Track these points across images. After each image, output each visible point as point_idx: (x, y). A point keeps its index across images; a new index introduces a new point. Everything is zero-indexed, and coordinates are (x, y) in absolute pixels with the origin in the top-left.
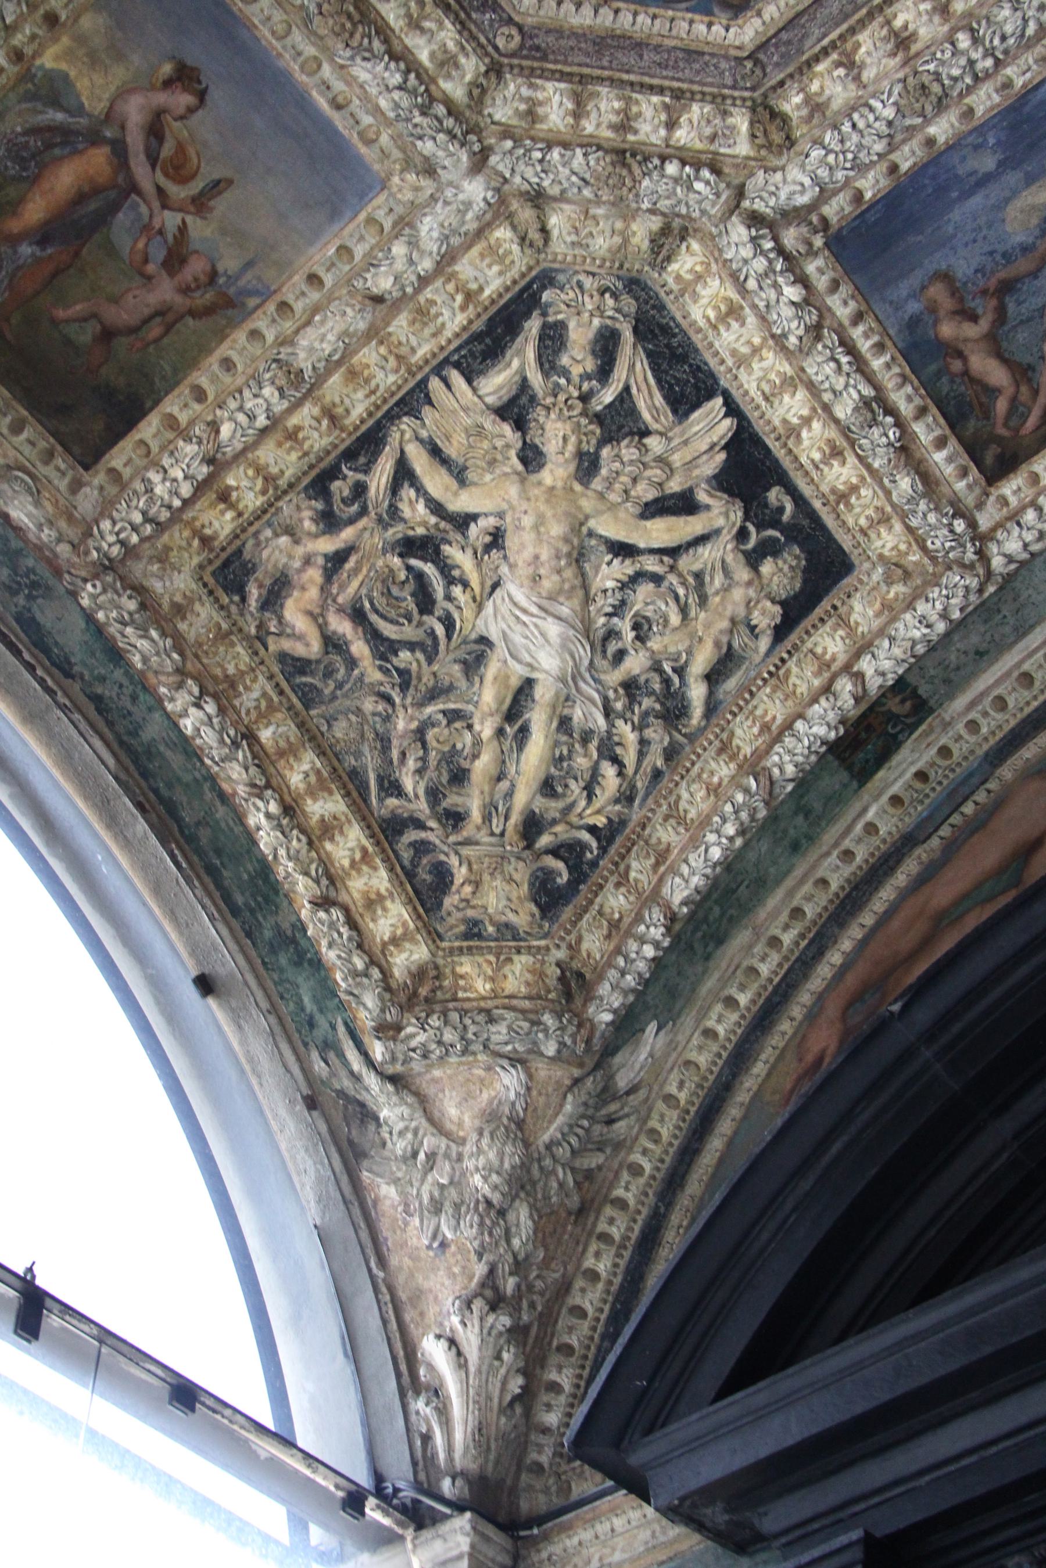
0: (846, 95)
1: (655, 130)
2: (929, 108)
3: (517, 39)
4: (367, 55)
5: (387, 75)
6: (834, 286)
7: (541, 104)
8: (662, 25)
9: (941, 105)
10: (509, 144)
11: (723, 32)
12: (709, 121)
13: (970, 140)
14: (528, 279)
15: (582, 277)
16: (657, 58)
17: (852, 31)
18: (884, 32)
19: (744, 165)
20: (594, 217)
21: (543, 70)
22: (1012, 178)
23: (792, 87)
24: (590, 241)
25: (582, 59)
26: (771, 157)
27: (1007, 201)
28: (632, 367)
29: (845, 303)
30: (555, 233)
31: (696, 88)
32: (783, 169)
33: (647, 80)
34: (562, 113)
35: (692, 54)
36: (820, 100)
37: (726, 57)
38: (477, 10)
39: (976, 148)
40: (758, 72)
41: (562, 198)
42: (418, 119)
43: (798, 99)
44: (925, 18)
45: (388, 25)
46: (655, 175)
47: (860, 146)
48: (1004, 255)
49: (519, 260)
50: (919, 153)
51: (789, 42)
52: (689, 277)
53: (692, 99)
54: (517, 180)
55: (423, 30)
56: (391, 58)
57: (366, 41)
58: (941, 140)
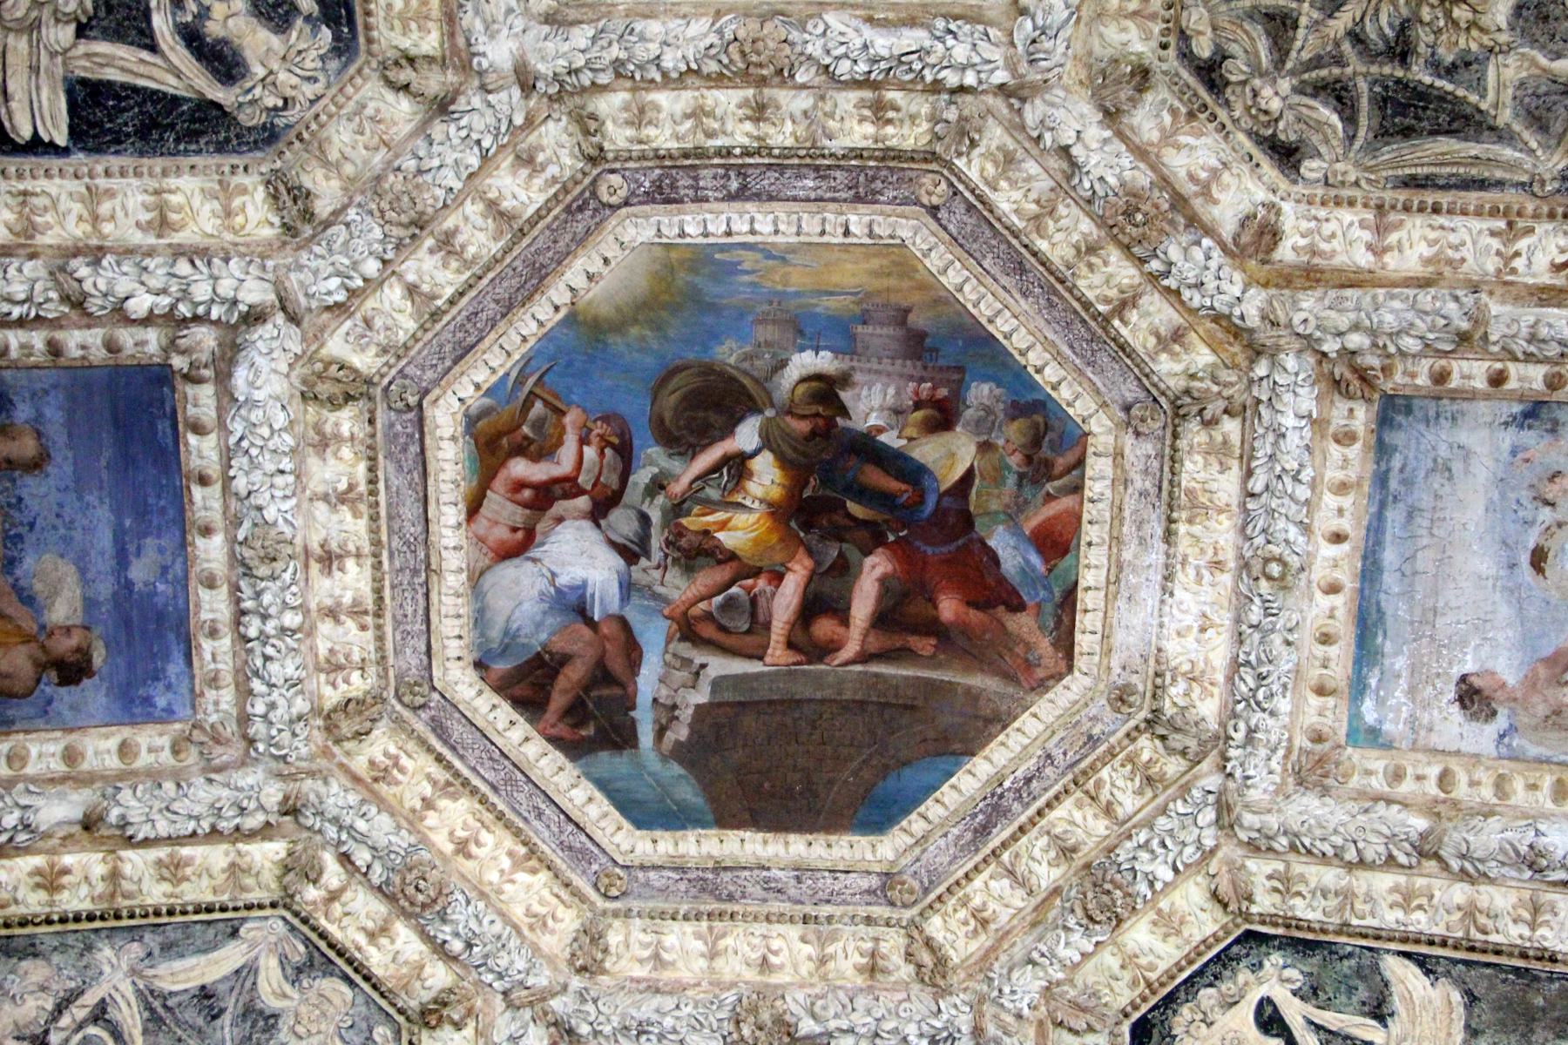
0: (316, 478)
1: (419, 272)
2: (247, 553)
3: (605, 198)
4: (713, 51)
5: (679, 55)
6: (112, 347)
7: (530, 177)
8: (512, 343)
9: (236, 561)
10: (519, 120)
11: (461, 395)
12: (388, 329)
13: (178, 567)
14: (360, 28)
15: (319, 88)
16: (484, 316)
17: (374, 518)
18: (351, 547)
19: (318, 336)
20: (377, 149)
21: (558, 202)
22: (105, 589)
23: (361, 431)
24: (354, 125)
25: (540, 244)
26: (305, 371)
27: (82, 571)
28: (178, 74)
29: (83, 347)
30: (390, 96)
31: (429, 335)
32: (287, 376)
33: (473, 293)
34: (507, 193)
35: (464, 352)
36: (328, 450)
37: (436, 382)
38: (660, 179)
39: (165, 570)
40: (400, 405)
41: (422, 129)
42: (616, 52)
43: (345, 430)
44: (338, 592)
45: (718, 87)
46: (377, 247)
47: (254, 465)
48: (20, 537)
49: (389, 37)
50: (203, 513)
51: (405, 450)
52: (237, 202)
53: (422, 326)
54: (477, 102)
55: (687, 116)
56: (689, 70)
57: (726, 61)
58: (200, 542)
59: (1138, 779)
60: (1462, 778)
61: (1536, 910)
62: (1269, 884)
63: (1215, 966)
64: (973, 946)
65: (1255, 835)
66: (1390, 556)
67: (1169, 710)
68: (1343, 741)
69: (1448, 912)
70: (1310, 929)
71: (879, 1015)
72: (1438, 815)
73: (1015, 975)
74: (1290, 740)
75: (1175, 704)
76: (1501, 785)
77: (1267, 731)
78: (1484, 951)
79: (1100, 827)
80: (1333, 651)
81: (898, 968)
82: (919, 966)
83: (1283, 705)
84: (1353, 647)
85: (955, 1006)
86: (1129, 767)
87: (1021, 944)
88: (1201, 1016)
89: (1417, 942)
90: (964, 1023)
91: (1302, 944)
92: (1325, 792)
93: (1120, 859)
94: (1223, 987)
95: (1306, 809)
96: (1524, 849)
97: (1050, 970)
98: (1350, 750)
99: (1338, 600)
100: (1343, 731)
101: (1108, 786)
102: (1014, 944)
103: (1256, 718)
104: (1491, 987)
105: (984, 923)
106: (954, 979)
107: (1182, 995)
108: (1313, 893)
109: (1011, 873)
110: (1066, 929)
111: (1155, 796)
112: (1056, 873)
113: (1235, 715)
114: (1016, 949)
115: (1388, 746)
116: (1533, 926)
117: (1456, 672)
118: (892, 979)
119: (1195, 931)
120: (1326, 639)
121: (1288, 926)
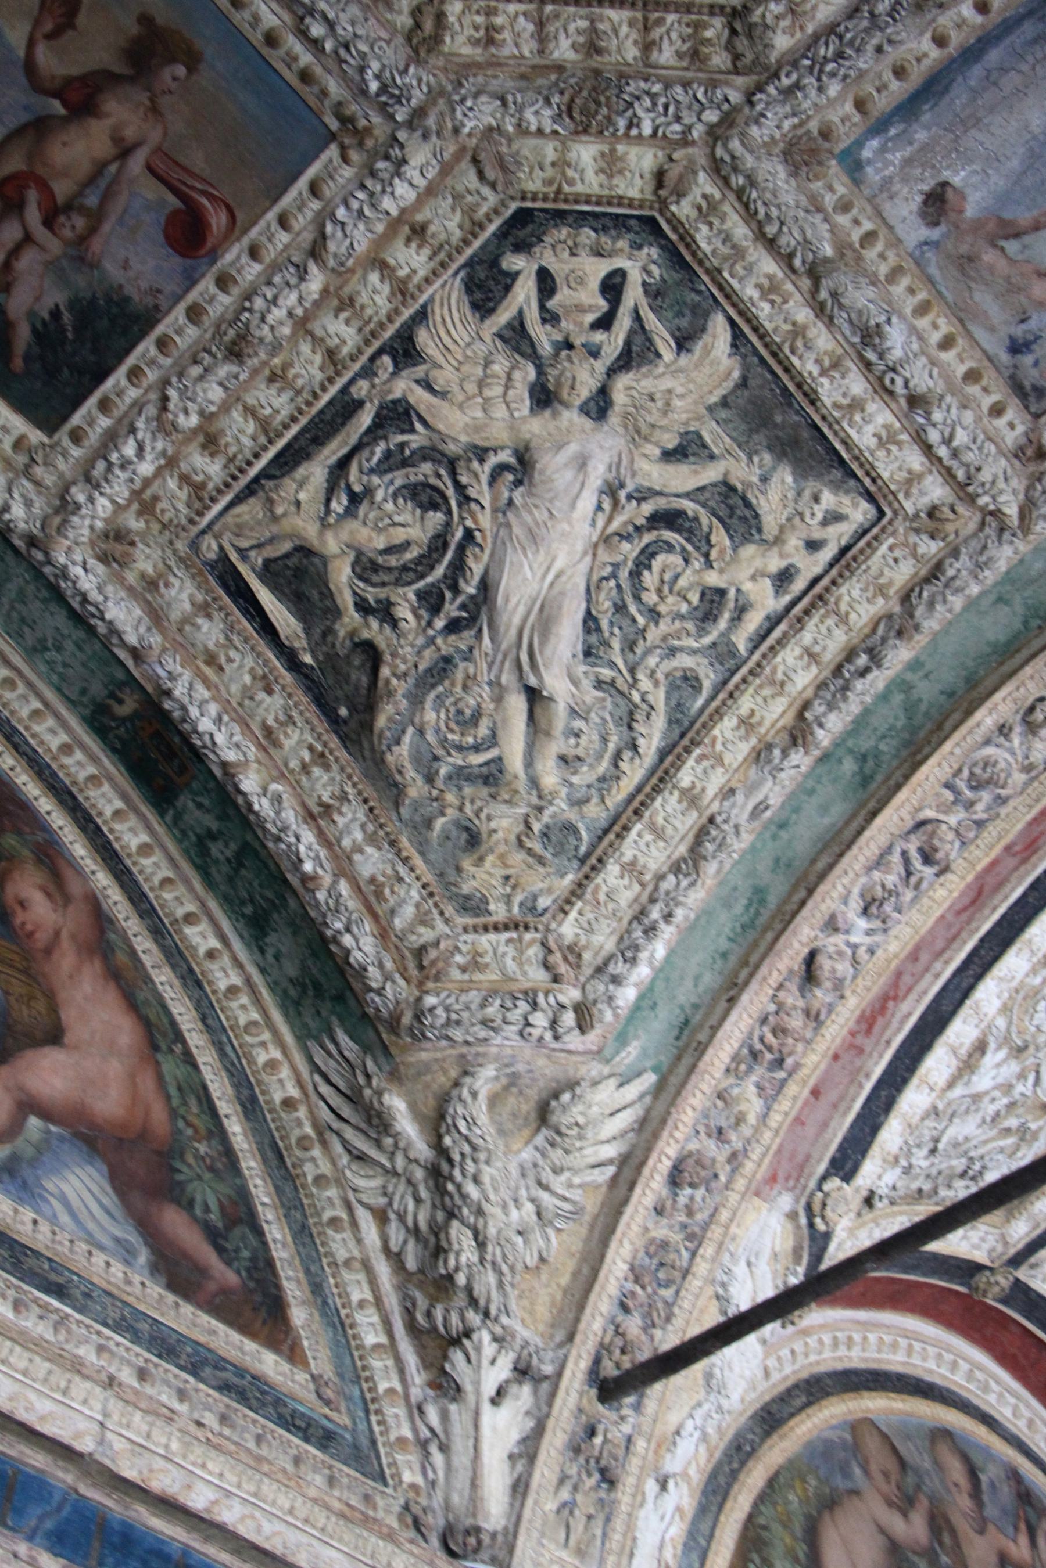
59: (688, 45)
60: (879, 246)
61: (836, 365)
62: (699, 199)
63: (611, 221)
64: (467, 50)
65: (727, 159)
66: (994, 56)
67: (755, 17)
68: (837, 151)
69: (785, 321)
70: (694, 254)
71: (360, 32)
72: (843, 255)
73: (484, 98)
74: (809, 117)
75: (763, 16)
76: (895, 273)
77: (806, 97)
78: (780, 362)
79: (632, 53)
80: (895, 85)
81: (400, 12)
82: (418, 26)
83: (834, 89)
84: (906, 96)
85: (420, 80)
86: (690, 31)
87: (502, 81)
88: (570, 243)
89: (748, 321)
90: (418, 97)
91: (680, 256)
92: (794, 173)
93: (628, 89)
94: (604, 239)
95: (775, 174)
96: (872, 323)
97: (507, 119)
98: (834, 162)
99: (935, 53)
100: (842, 145)
101: (663, 29)
102: (495, 77)
103: (810, 81)
104: (761, 387)
105: (490, 41)
106: (432, 61)
107: (570, 219)
108: (720, 231)
109: (541, 24)
110: (547, 101)
111: (687, 69)
112: (571, 55)
113: (795, 64)
114: (494, 82)
115: (857, 182)
116: (823, 373)
117: (946, 175)
118: (389, 16)
119: (622, 186)
120: (899, 72)
121: (682, 238)
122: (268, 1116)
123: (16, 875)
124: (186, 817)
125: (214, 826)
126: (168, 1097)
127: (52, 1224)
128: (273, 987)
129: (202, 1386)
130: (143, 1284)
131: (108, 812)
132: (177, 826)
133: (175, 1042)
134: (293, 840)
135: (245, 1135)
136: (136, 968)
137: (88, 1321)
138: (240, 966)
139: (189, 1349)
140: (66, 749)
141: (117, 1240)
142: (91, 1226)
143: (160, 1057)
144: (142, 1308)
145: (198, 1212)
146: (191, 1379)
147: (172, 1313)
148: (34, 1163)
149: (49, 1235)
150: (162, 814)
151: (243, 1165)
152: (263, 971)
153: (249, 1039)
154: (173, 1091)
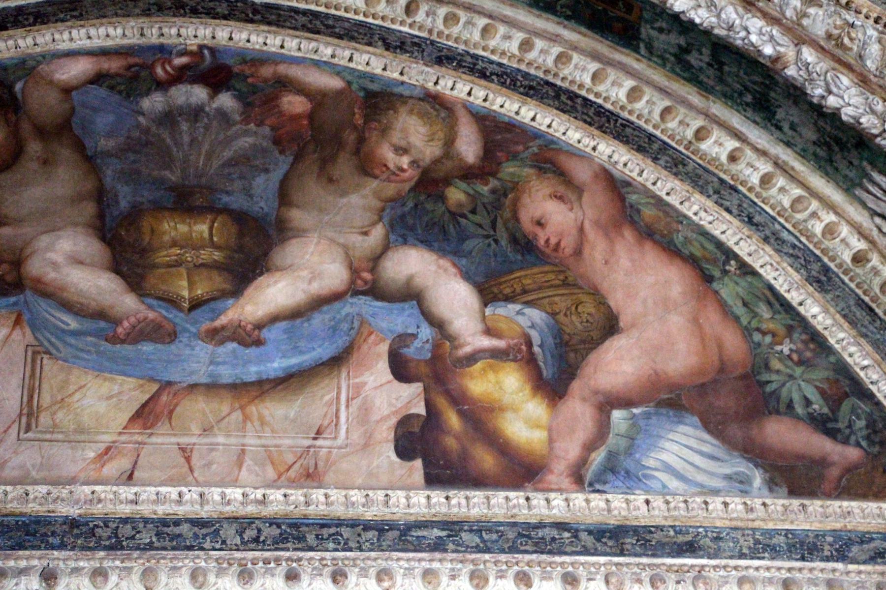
122: (846, 279)
123: (526, 200)
124: (656, 44)
125: (682, 42)
126: (737, 319)
127: (664, 495)
128: (803, 154)
129: (851, 567)
130: (764, 504)
131: (587, 80)
132: (652, 53)
133: (727, 262)
134: (743, 34)
135: (826, 311)
136: (666, 214)
137: (724, 562)
138: (763, 153)
139: (830, 539)
140: (526, 46)
141: (728, 478)
142: (700, 478)
143: (715, 285)
144: (771, 526)
145: (799, 410)
146: (840, 566)
147: (801, 516)
148: (629, 451)
149: (664, 507)
150: (636, 50)
151: (832, 341)
152: (788, 144)
153: (799, 216)
154: (740, 310)
